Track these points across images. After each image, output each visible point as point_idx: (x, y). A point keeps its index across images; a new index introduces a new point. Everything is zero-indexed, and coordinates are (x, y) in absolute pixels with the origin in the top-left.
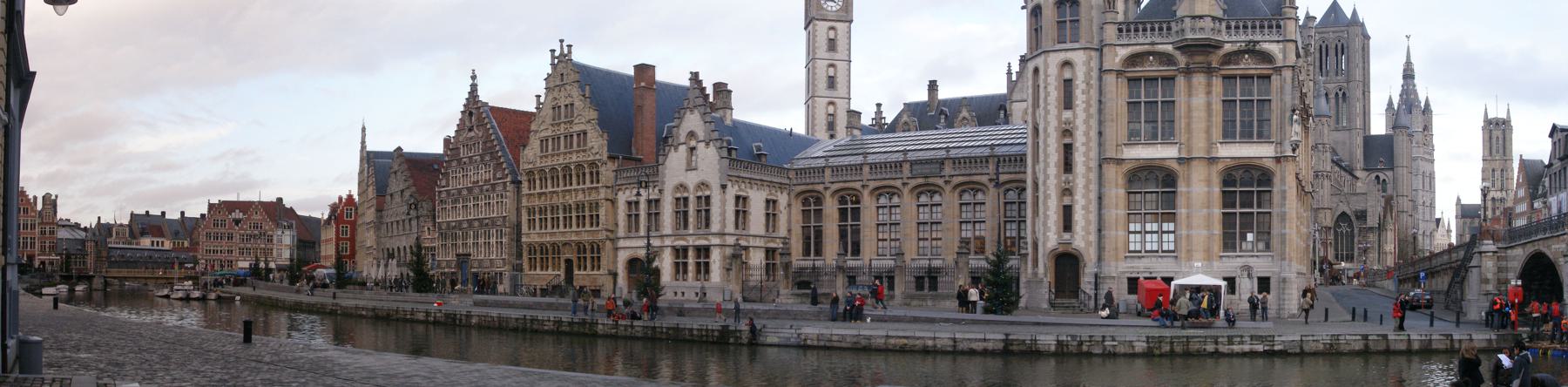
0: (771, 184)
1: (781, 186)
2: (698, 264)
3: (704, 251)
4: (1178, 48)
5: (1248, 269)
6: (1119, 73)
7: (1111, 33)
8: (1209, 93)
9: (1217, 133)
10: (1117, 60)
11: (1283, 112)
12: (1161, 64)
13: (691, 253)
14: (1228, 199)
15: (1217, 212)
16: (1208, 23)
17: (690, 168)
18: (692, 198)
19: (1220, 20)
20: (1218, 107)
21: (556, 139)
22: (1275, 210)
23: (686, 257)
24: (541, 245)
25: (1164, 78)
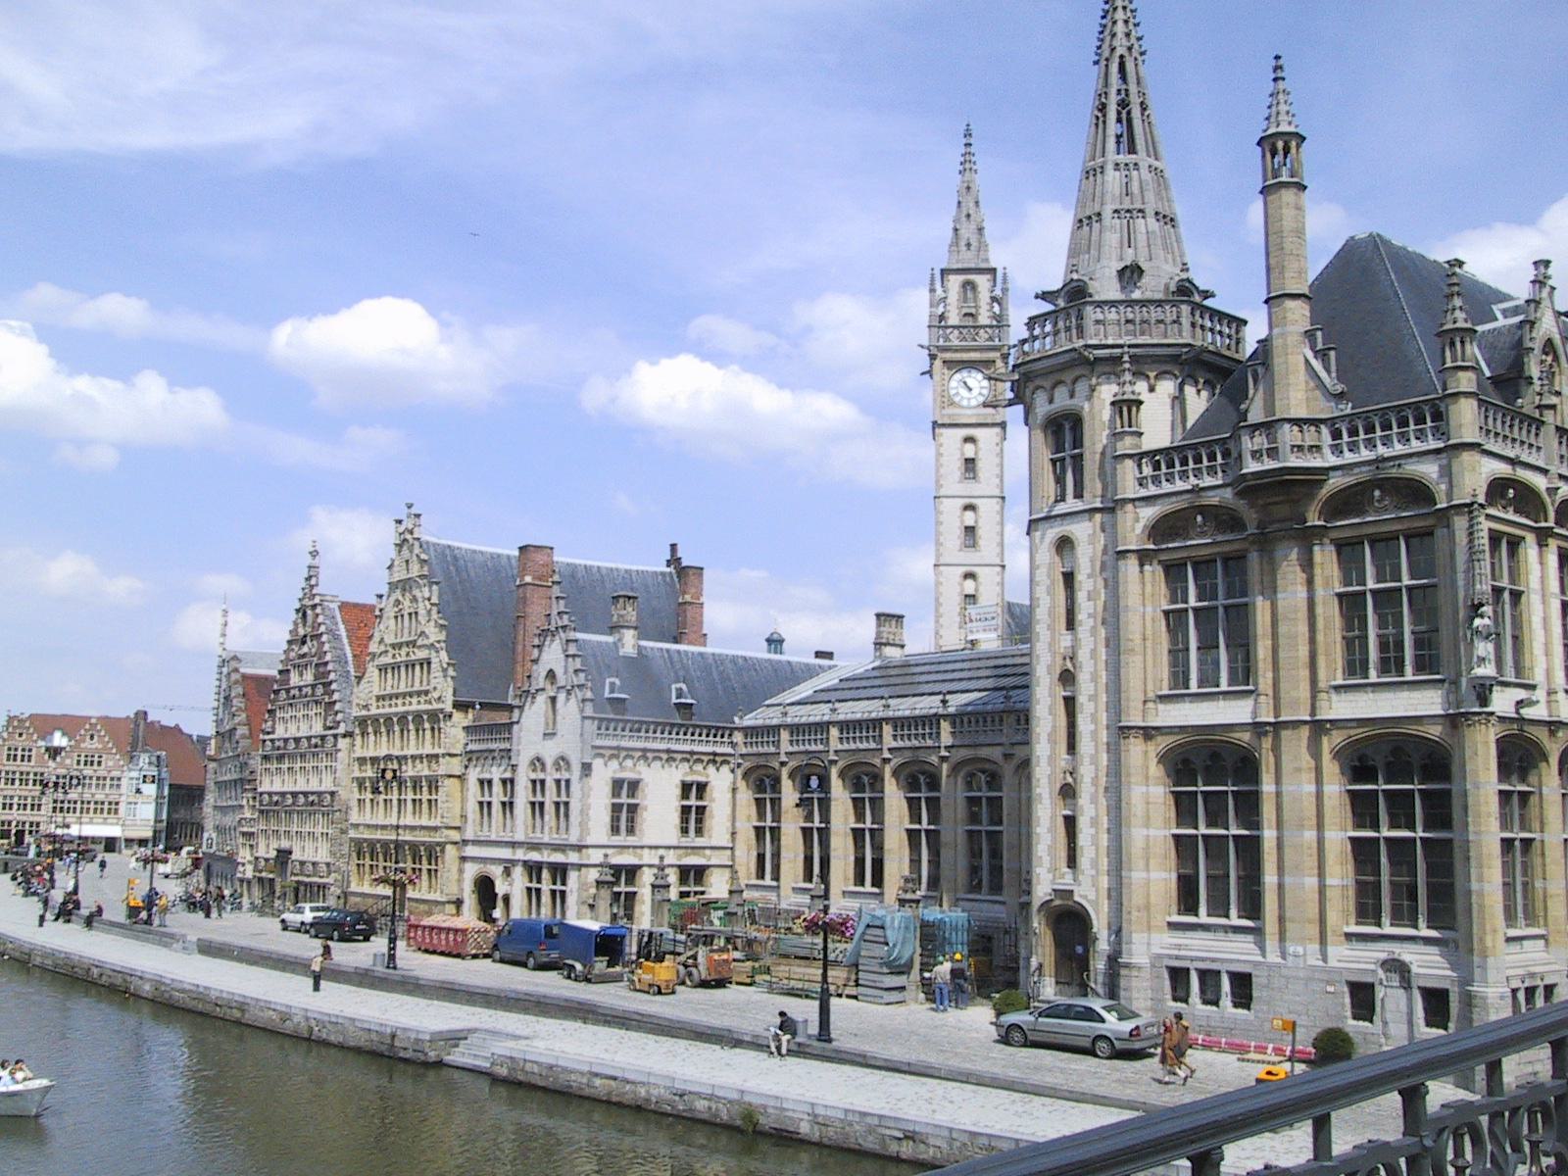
0: (691, 757)
1: (715, 759)
2: (553, 892)
3: (560, 872)
6: (1144, 556)
9: (1332, 669)
10: (1139, 528)
14: (1362, 808)
16: (1288, 435)
18: (550, 785)
19: (1315, 422)
20: (1330, 613)
21: (395, 667)
23: (539, 881)
24: (372, 844)
25: (1227, 559)
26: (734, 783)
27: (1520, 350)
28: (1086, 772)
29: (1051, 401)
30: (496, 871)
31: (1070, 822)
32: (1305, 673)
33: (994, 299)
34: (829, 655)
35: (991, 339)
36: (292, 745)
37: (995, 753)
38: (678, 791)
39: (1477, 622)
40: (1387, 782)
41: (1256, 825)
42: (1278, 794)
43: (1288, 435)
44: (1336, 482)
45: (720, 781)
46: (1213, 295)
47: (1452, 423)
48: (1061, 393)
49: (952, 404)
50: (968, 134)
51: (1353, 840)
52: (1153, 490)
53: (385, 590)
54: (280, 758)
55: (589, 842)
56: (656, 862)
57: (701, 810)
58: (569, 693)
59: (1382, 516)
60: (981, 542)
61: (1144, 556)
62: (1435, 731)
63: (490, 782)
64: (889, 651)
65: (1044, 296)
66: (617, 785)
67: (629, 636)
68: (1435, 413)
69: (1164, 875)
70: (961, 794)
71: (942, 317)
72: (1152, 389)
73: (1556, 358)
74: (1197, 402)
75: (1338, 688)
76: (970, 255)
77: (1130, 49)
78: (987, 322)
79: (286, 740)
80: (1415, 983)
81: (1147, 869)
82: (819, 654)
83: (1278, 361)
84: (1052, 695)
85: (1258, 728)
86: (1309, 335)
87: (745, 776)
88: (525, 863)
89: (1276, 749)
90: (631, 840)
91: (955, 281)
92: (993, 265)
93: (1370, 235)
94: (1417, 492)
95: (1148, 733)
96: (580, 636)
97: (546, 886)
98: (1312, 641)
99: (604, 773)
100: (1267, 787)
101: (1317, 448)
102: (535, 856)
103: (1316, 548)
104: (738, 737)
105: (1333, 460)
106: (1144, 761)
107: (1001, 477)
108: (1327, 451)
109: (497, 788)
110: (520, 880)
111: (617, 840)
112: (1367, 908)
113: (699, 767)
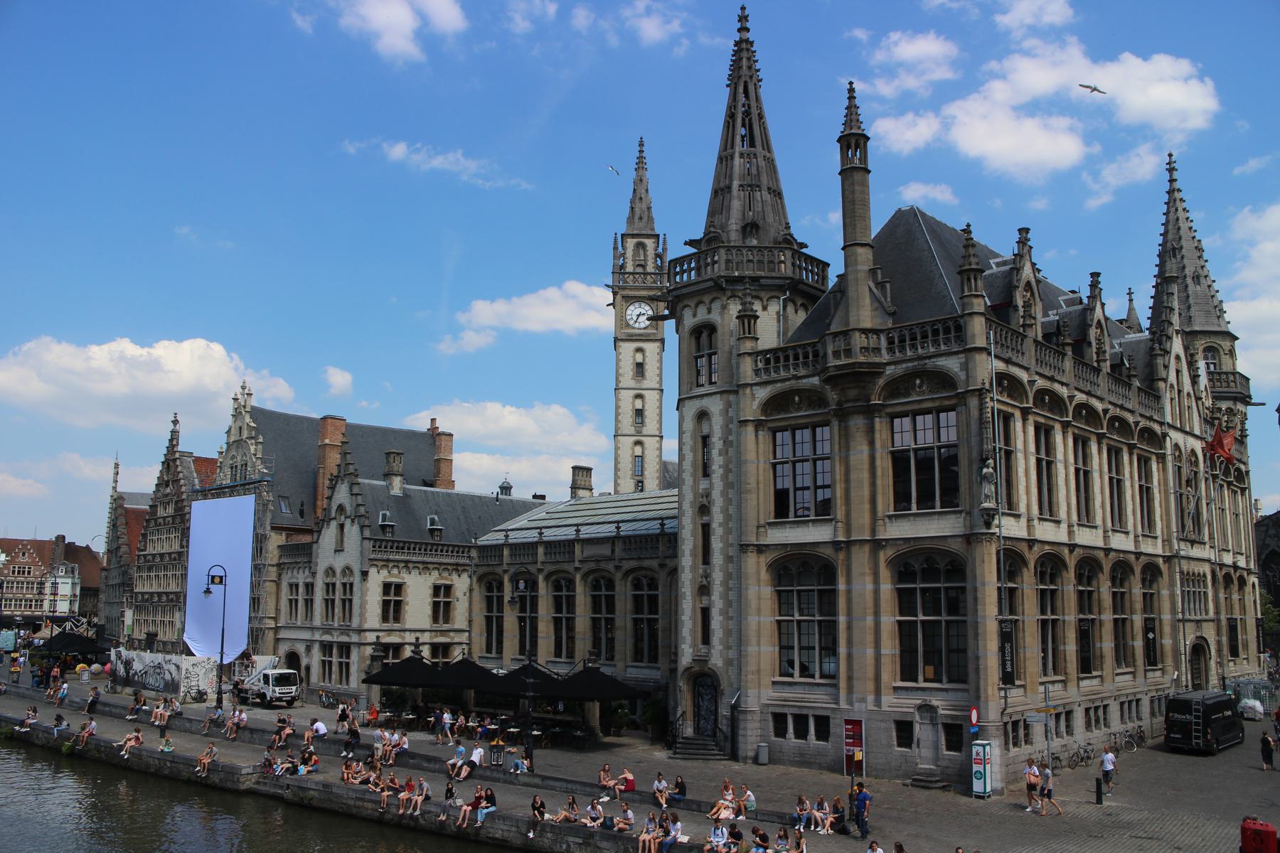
0: (439, 566)
1: (458, 569)
2: (341, 664)
3: (345, 649)
4: (827, 381)
5: (926, 709)
6: (758, 424)
7: (747, 369)
8: (872, 443)
9: (886, 502)
10: (756, 404)
11: (970, 463)
12: (811, 405)
13: (335, 651)
14: (905, 601)
15: (889, 620)
17: (339, 550)
18: (338, 586)
19: (876, 332)
20: (885, 465)
22: (969, 619)
23: (331, 656)
26: (471, 585)
27: (1010, 289)
28: (717, 577)
29: (695, 316)
30: (301, 649)
31: (706, 613)
32: (867, 506)
33: (657, 256)
34: (543, 497)
35: (655, 282)
36: (158, 559)
37: (654, 564)
38: (431, 591)
39: (985, 470)
40: (924, 581)
41: (834, 613)
42: (849, 592)
43: (859, 340)
44: (890, 370)
45: (461, 584)
46: (806, 246)
47: (969, 333)
48: (702, 311)
49: (628, 325)
50: (641, 144)
51: (899, 622)
52: (765, 377)
53: (225, 446)
54: (150, 569)
55: (366, 626)
56: (414, 641)
57: (447, 604)
58: (353, 521)
59: (920, 395)
60: (647, 420)
61: (758, 424)
62: (956, 546)
63: (297, 586)
64: (581, 493)
65: (691, 243)
66: (387, 587)
67: (397, 481)
68: (955, 329)
69: (771, 649)
70: (630, 592)
71: (622, 267)
72: (765, 308)
73: (1033, 294)
74: (798, 318)
75: (890, 517)
76: (641, 225)
77: (751, 77)
78: (653, 270)
79: (154, 556)
80: (939, 721)
81: (759, 645)
82: (535, 497)
83: (851, 292)
84: (694, 523)
85: (836, 545)
86: (873, 272)
87: (480, 579)
88: (321, 642)
89: (848, 558)
90: (397, 626)
91: (631, 243)
92: (657, 232)
93: (912, 208)
94: (944, 380)
95: (760, 549)
96: (360, 480)
97: (335, 659)
98: (873, 484)
99: (377, 578)
100: (842, 586)
101: (877, 350)
102: (327, 638)
103: (877, 420)
104: (474, 553)
105: (885, 357)
106: (756, 568)
107: (660, 375)
108: (884, 352)
109: (301, 590)
110: (316, 657)
111: (386, 626)
112: (908, 672)
113: (445, 574)
